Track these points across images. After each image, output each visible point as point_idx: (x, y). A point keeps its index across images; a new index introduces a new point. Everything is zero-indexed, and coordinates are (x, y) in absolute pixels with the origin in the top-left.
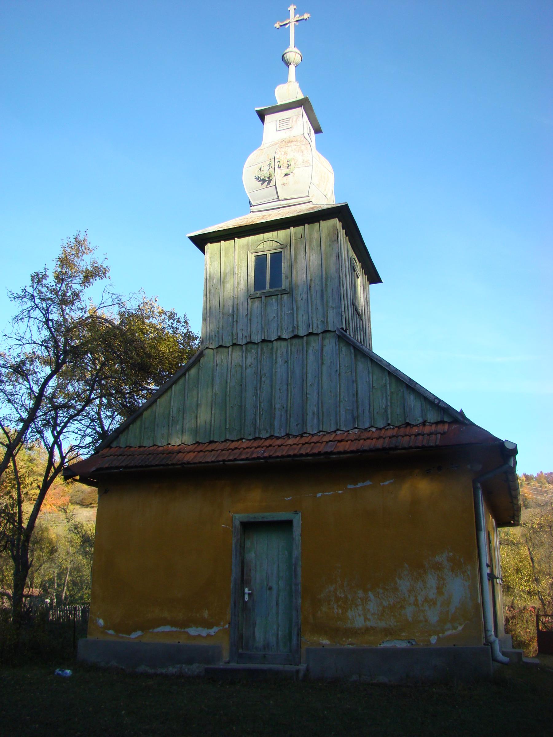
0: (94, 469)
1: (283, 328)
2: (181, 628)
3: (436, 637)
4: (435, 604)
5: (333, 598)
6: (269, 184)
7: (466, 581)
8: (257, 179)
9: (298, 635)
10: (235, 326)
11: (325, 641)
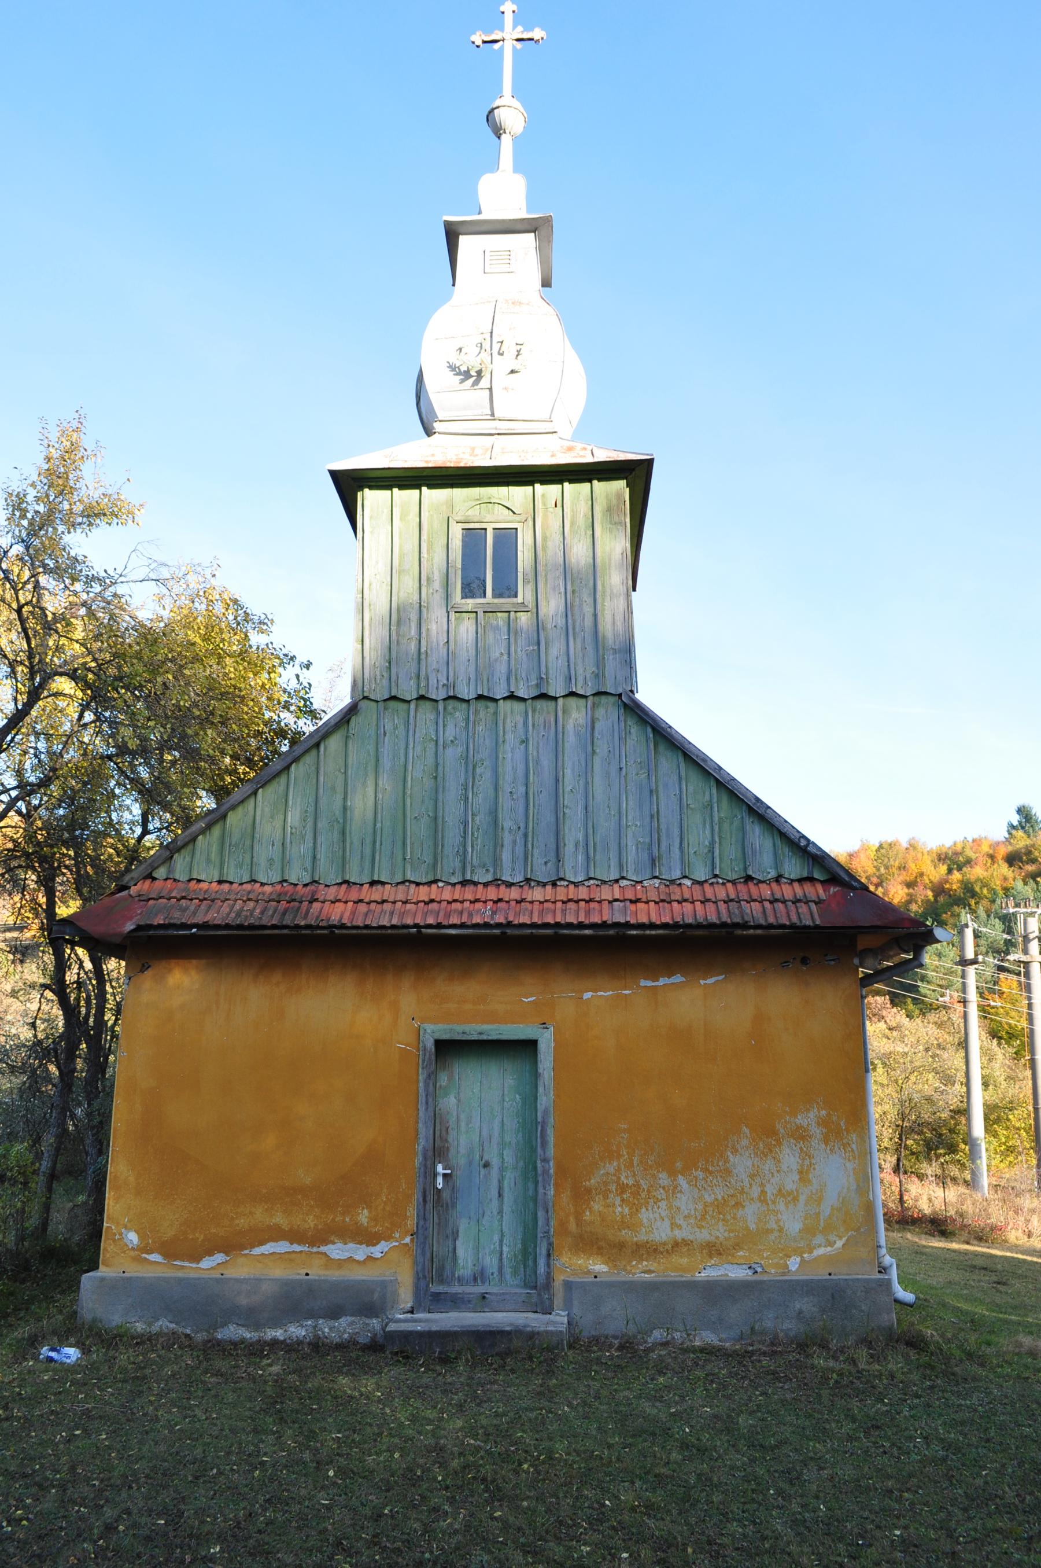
0: (130, 926)
1: (519, 676)
2: (312, 1244)
3: (798, 1259)
4: (795, 1199)
5: (613, 1187)
6: (476, 383)
7: (849, 1160)
8: (452, 368)
9: (549, 1255)
10: (423, 663)
11: (599, 1267)
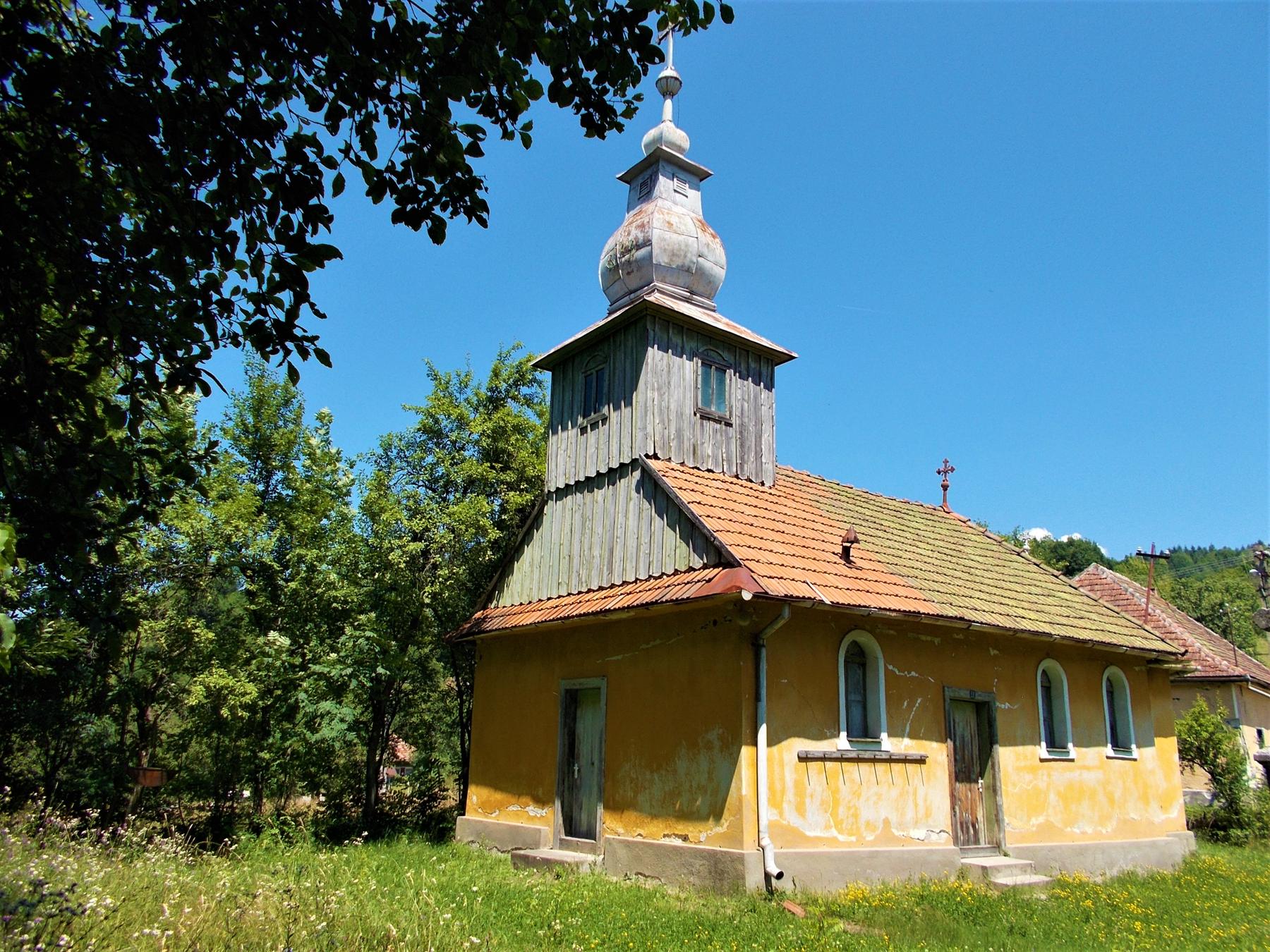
4: (706, 792)
